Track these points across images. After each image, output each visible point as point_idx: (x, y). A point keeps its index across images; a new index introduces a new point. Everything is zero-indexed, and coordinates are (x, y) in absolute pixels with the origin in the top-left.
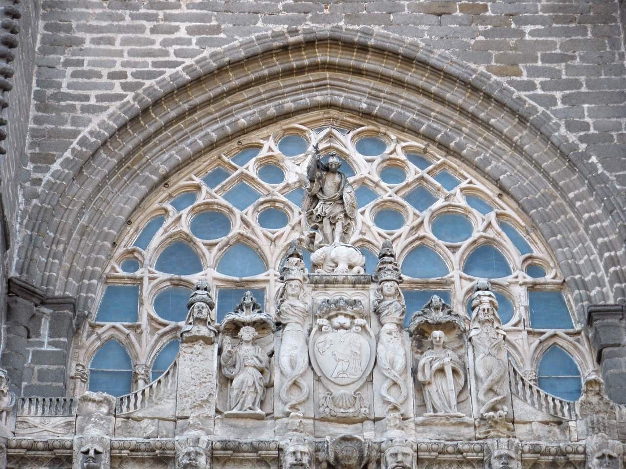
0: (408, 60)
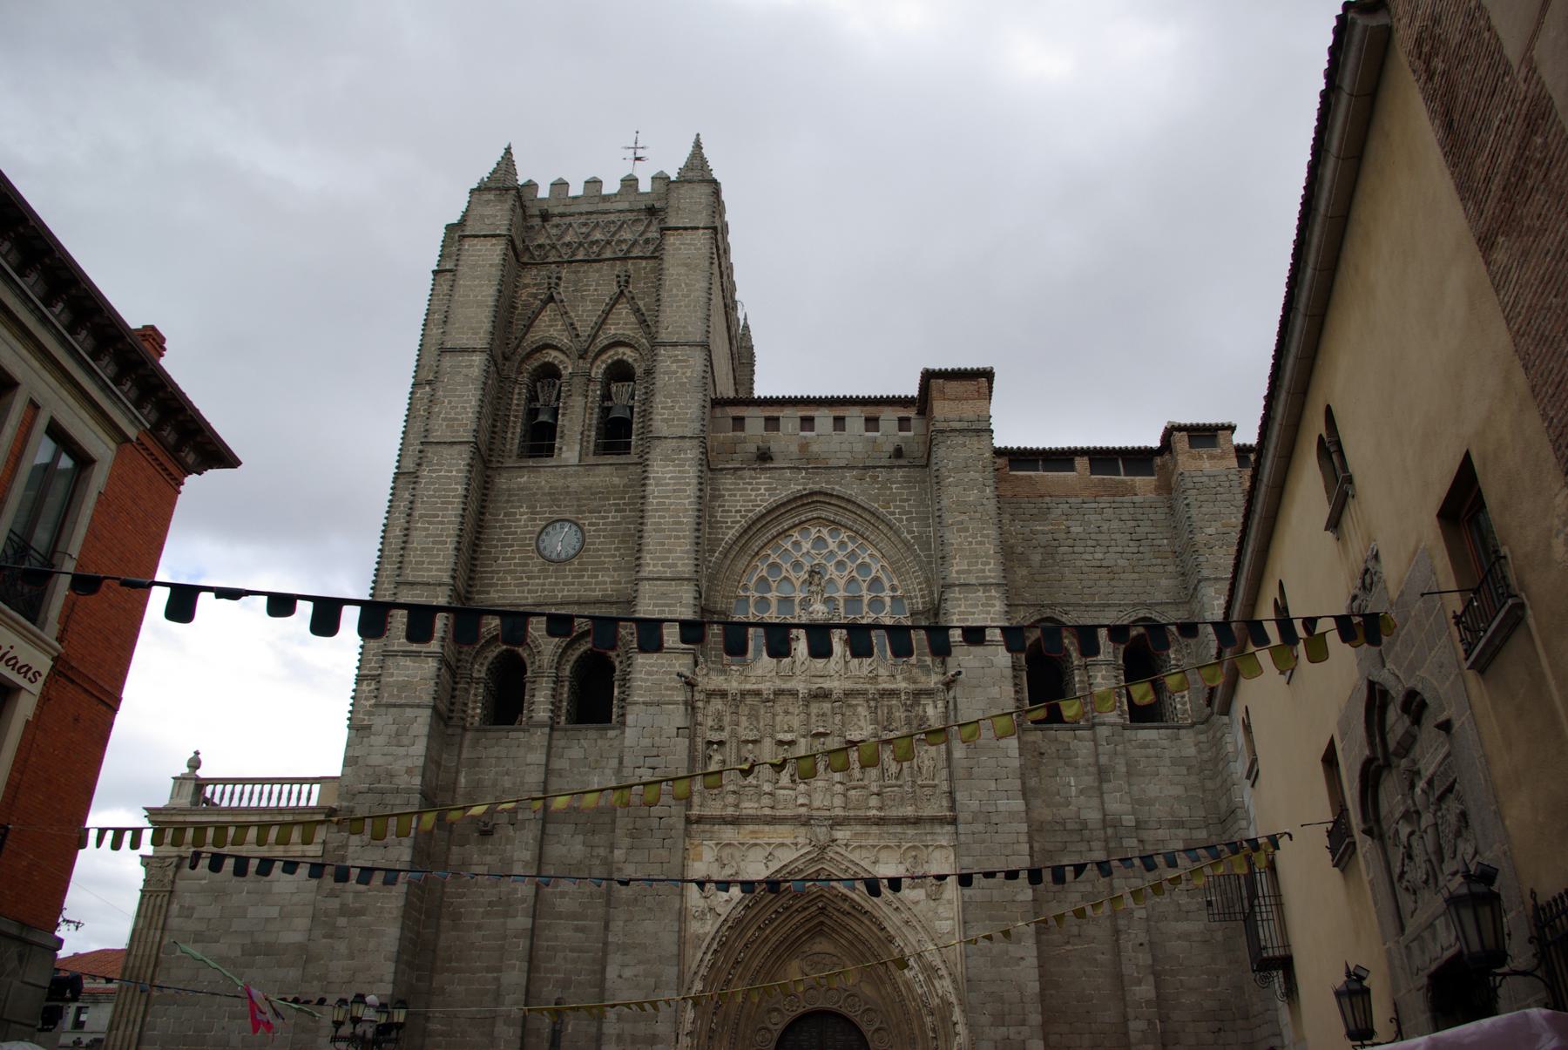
0: (849, 501)
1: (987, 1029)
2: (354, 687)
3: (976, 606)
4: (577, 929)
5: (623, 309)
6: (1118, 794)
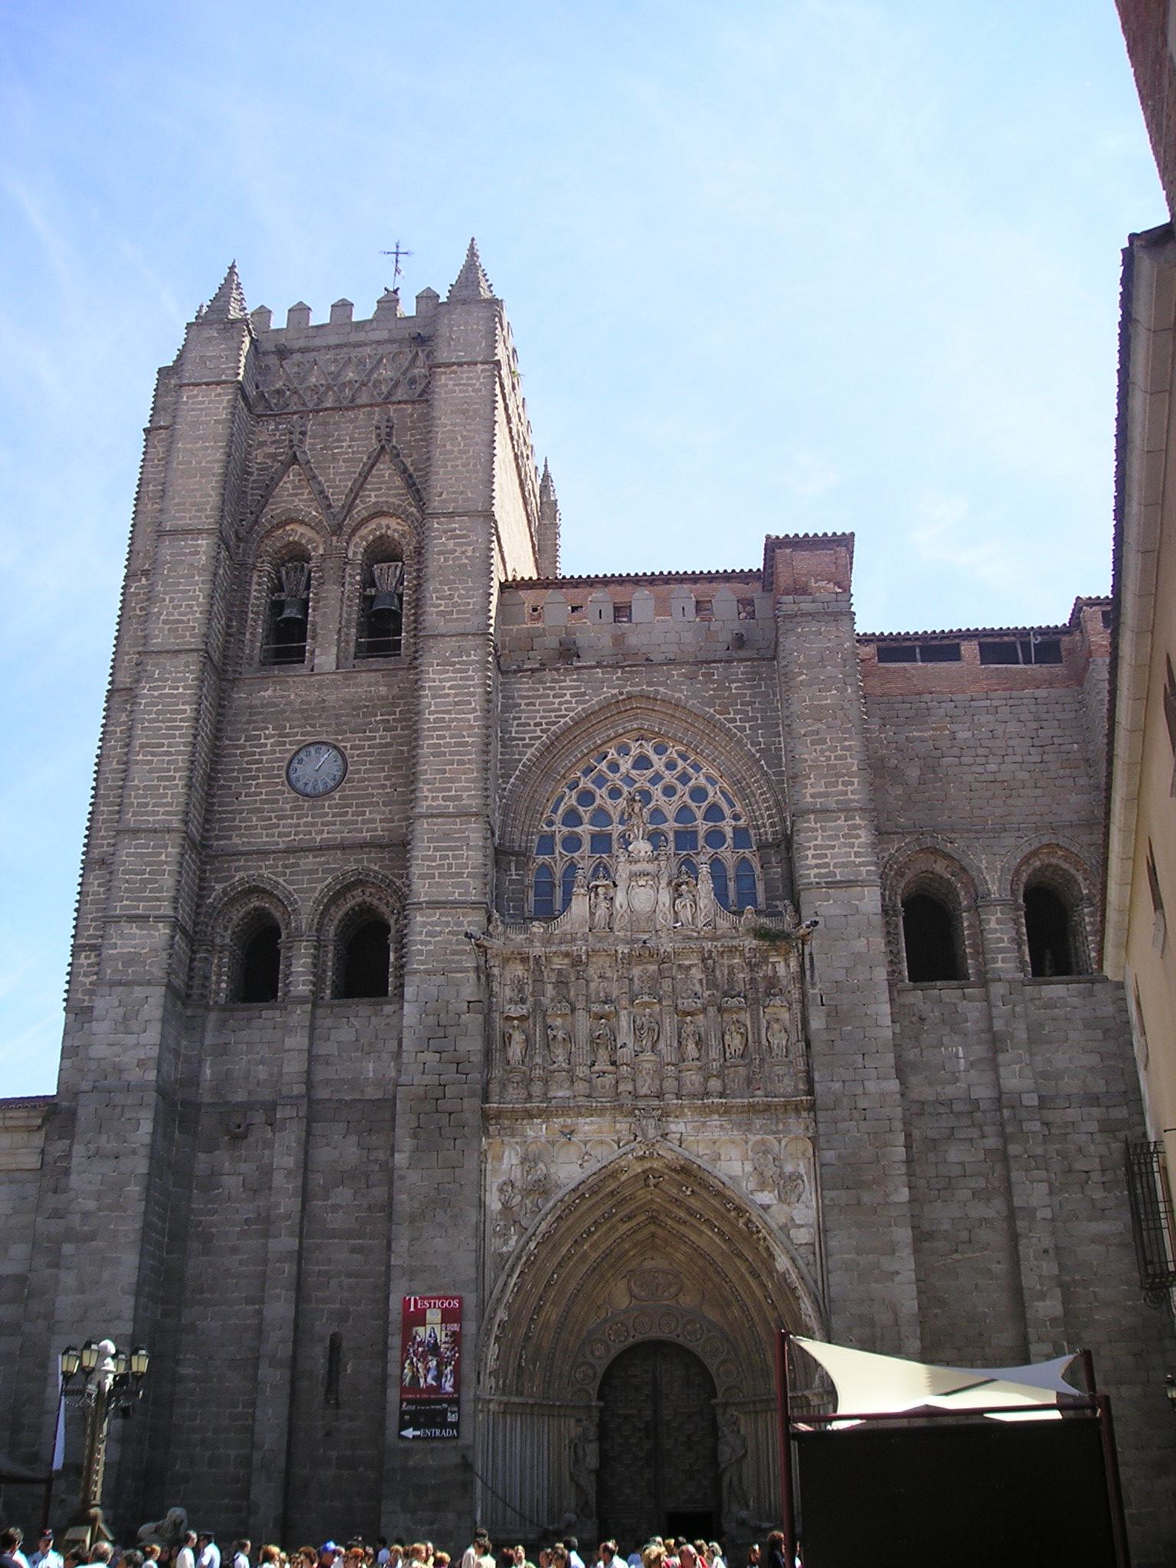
2: (70, 960)
3: (837, 837)
4: (353, 1250)
5: (385, 469)
6: (1017, 1067)
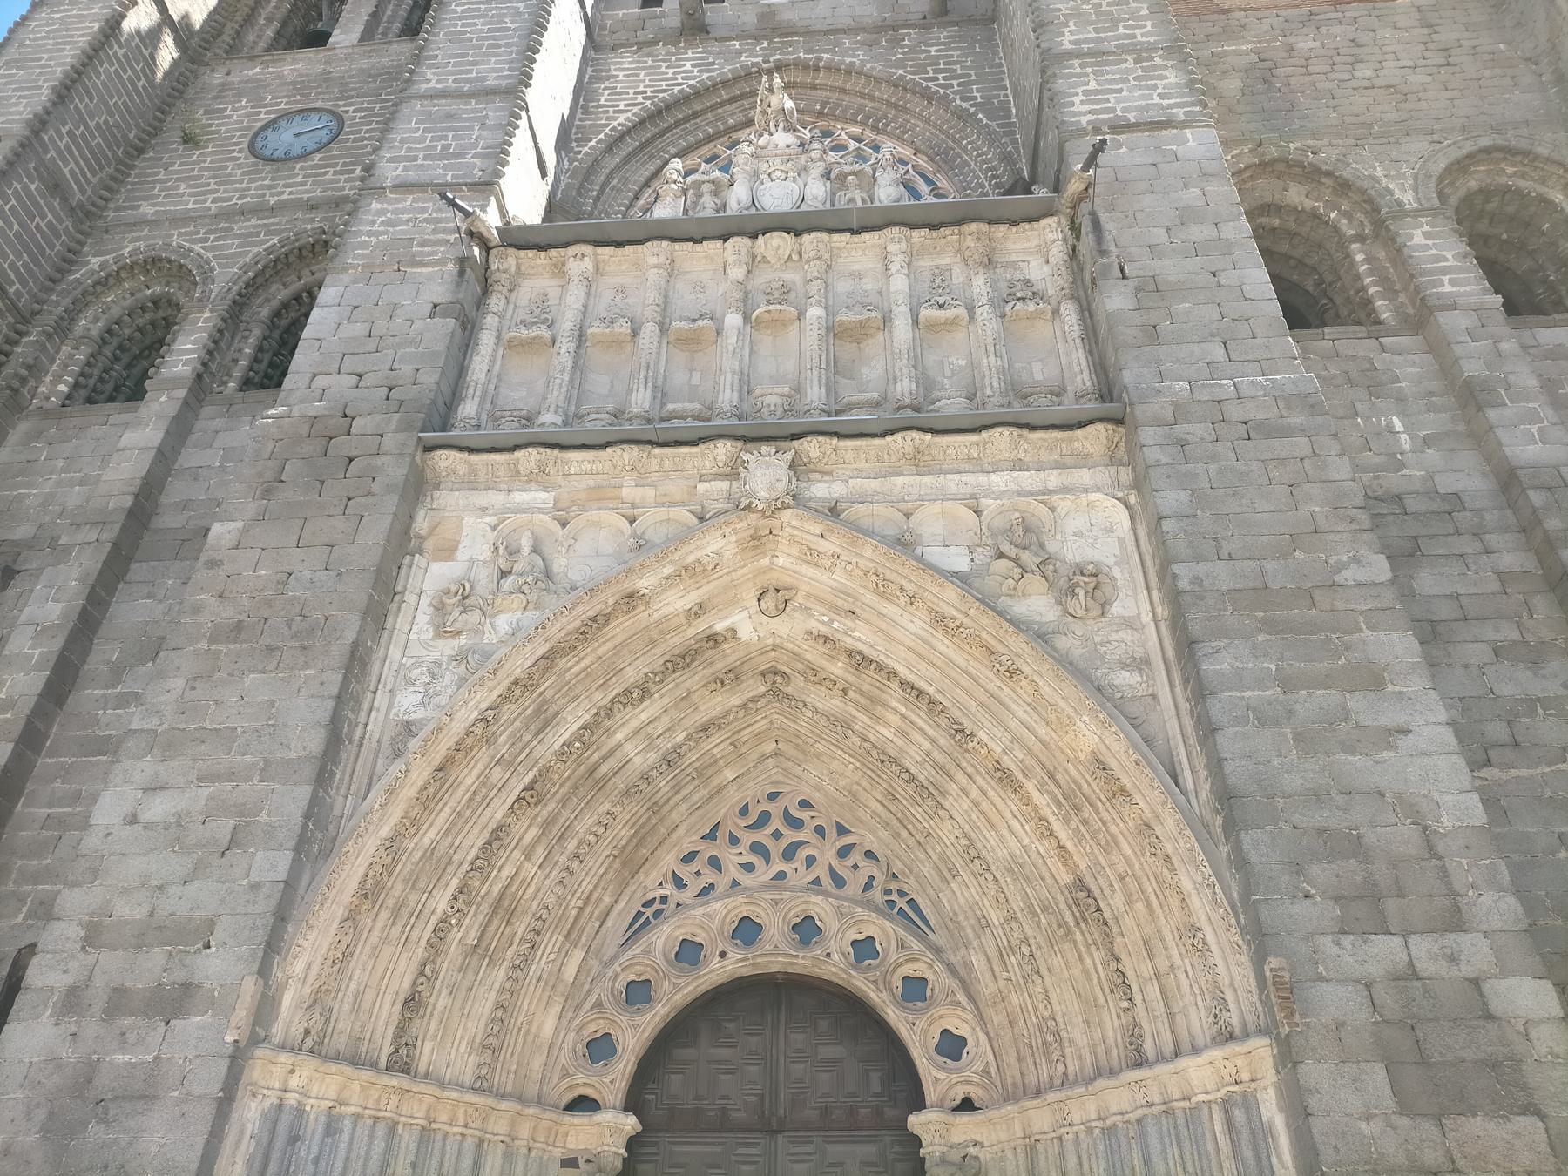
1: (1326, 943)
3: (1126, 80)
6: (1534, 429)
